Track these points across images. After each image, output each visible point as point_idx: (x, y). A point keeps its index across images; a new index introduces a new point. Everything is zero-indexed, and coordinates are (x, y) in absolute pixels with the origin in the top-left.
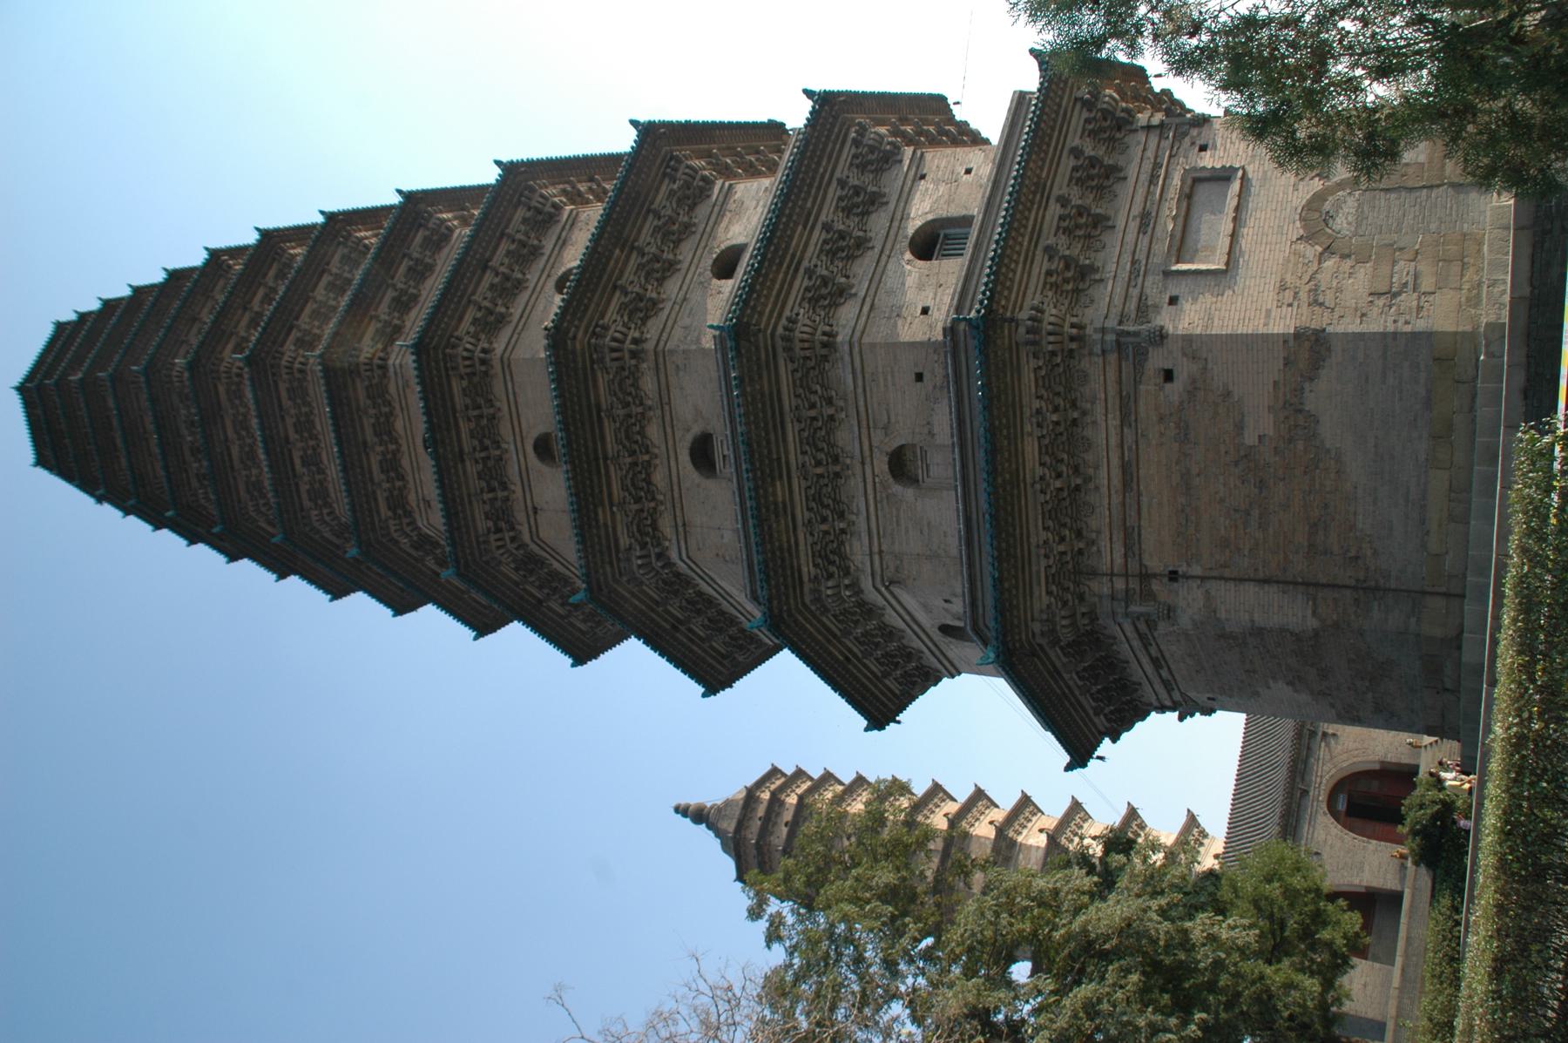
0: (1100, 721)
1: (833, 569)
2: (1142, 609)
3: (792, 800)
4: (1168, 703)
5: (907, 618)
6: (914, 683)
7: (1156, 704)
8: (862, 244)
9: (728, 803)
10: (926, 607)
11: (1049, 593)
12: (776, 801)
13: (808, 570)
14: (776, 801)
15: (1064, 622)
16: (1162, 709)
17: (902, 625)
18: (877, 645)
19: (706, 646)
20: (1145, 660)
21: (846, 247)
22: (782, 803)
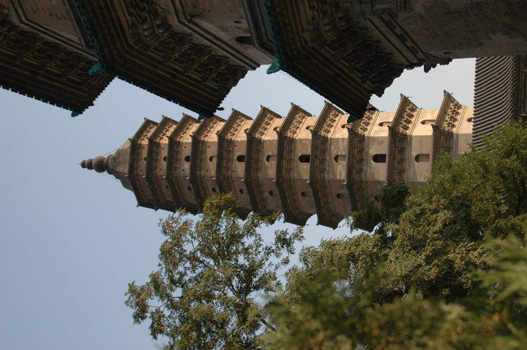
0: (368, 85)
1: (144, 14)
2: (385, 6)
3: (165, 141)
4: (415, 61)
5: (210, 37)
6: (227, 80)
7: (406, 63)
9: (120, 153)
10: (222, 28)
11: (312, 8)
12: (154, 145)
13: (125, 19)
14: (154, 145)
15: (327, 28)
16: (411, 66)
17: (208, 43)
18: (193, 60)
19: (64, 80)
20: (393, 38)
22: (158, 145)
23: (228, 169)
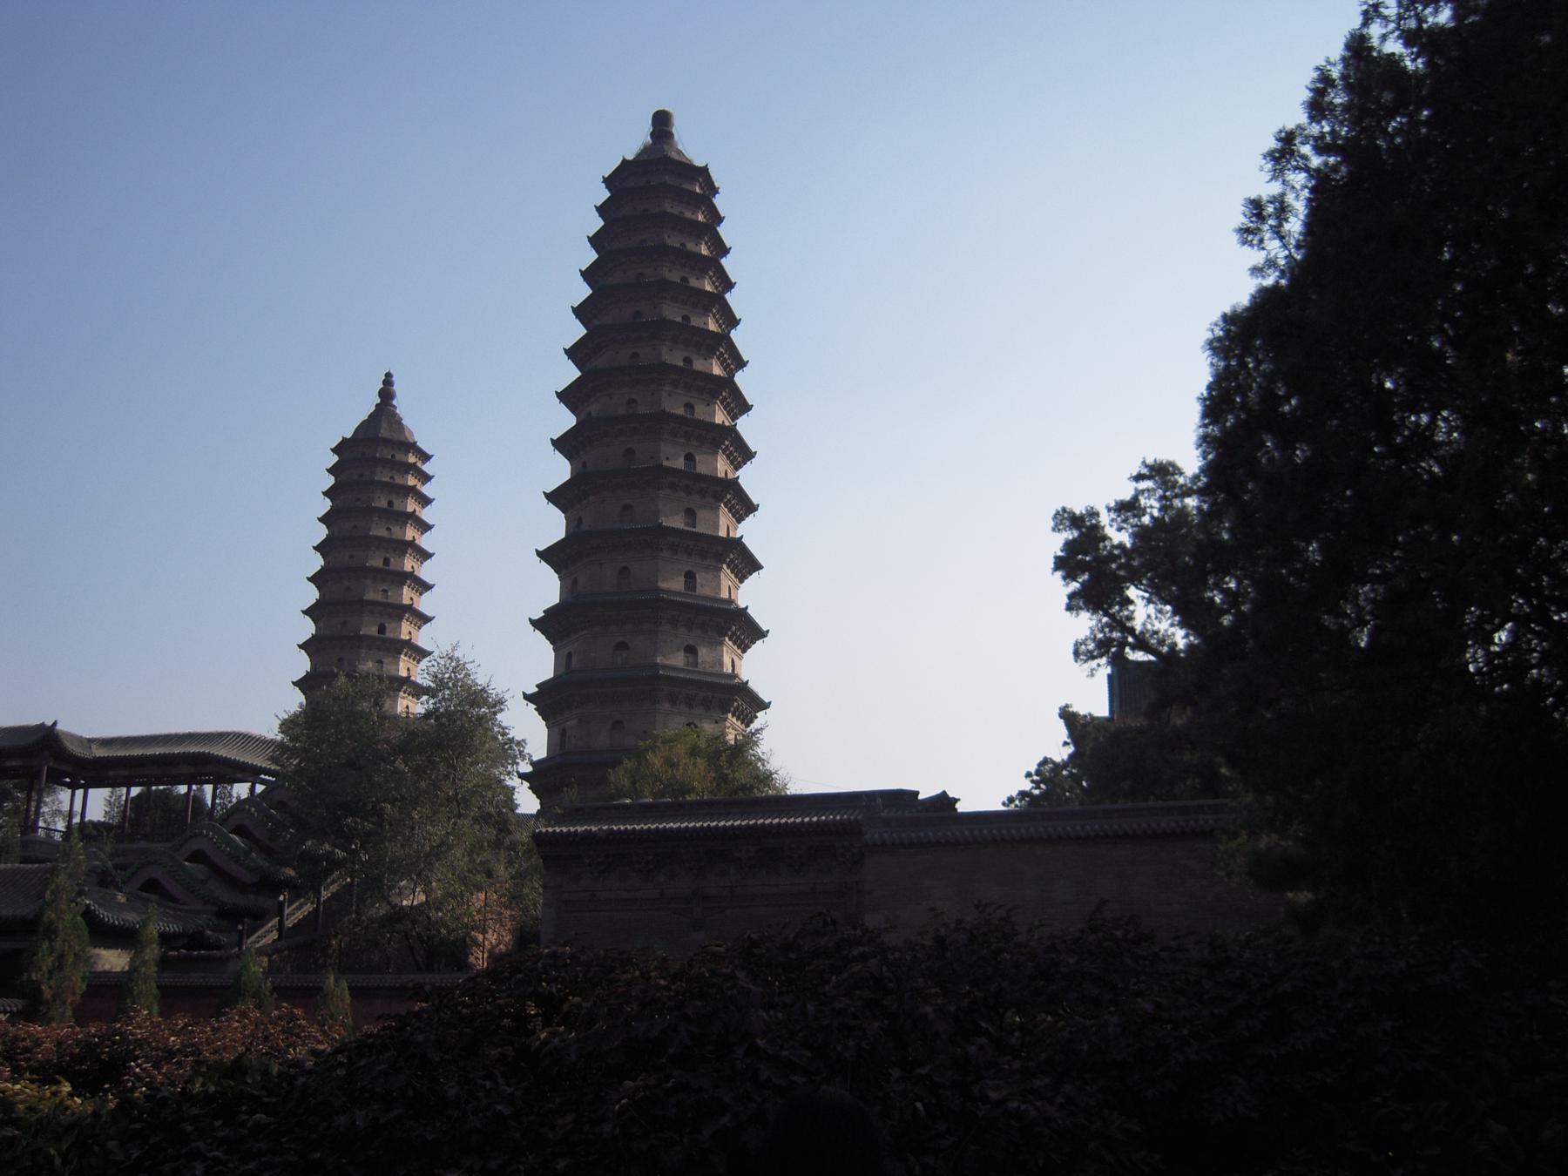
8: (691, 706)
21: (690, 703)
23: (378, 547)
